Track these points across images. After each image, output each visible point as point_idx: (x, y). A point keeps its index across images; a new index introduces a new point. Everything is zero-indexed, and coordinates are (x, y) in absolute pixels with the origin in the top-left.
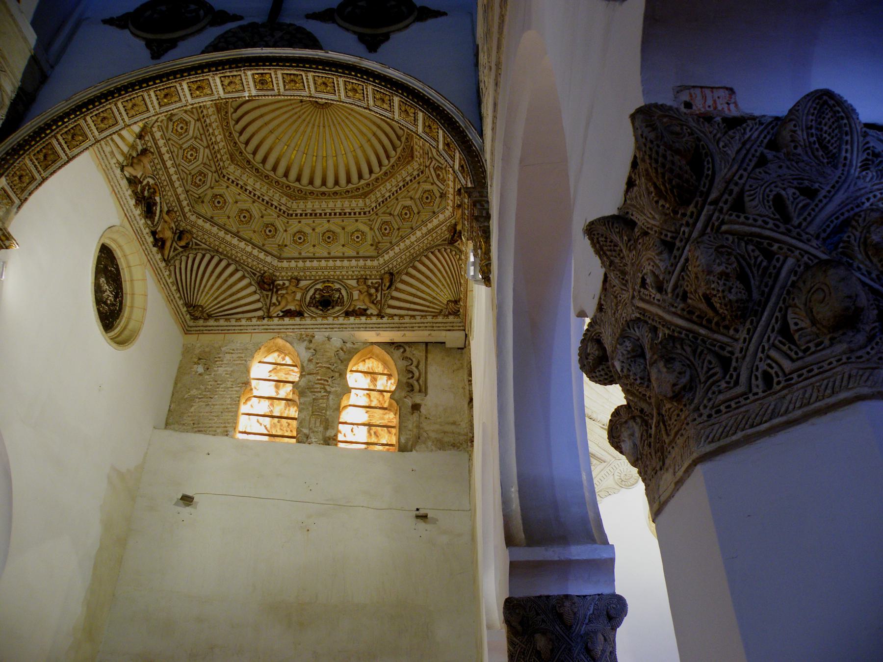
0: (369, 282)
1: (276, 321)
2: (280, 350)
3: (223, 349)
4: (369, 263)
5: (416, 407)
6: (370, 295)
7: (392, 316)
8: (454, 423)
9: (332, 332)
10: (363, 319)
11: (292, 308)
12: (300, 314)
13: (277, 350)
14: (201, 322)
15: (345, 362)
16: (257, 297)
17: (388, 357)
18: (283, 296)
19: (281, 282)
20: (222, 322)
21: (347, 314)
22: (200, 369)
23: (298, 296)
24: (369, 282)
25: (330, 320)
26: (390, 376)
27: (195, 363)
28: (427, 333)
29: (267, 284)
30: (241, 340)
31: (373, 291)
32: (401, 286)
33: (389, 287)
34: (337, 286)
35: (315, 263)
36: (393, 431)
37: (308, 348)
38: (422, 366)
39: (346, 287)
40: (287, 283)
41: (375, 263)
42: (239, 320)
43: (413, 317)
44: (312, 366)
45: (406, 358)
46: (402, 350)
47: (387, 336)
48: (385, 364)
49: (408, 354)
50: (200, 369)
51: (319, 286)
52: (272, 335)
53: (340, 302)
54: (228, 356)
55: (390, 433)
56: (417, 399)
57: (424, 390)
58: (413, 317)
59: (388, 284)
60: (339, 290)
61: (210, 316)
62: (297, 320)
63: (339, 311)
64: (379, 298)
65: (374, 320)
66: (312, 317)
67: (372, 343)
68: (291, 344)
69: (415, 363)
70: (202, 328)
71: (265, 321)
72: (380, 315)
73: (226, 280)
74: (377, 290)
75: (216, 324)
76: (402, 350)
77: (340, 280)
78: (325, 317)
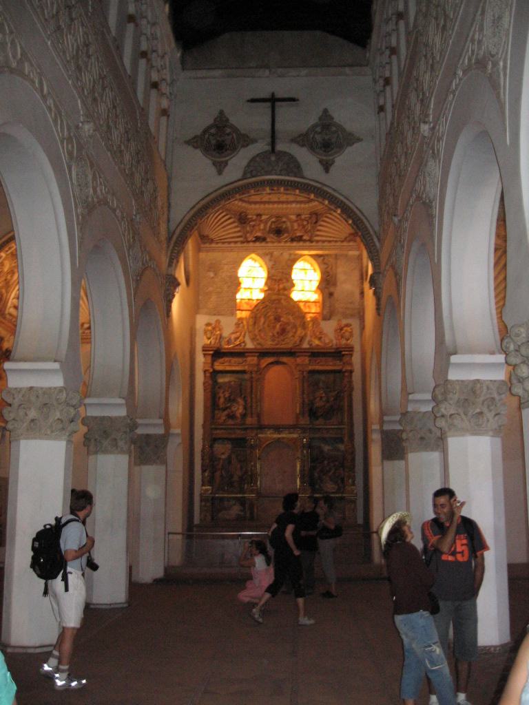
0: (303, 217)
1: (251, 244)
4: (303, 206)
5: (331, 294)
6: (304, 227)
7: (317, 241)
8: (351, 303)
9: (280, 249)
10: (301, 244)
11: (259, 234)
12: (264, 240)
13: (250, 258)
14: (207, 245)
15: (290, 267)
16: (238, 229)
18: (254, 226)
19: (250, 216)
20: (219, 245)
21: (292, 240)
22: (212, 274)
23: (262, 226)
24: (303, 217)
25: (282, 244)
29: (243, 219)
30: (232, 256)
31: (305, 223)
32: (322, 223)
33: (316, 222)
34: (284, 219)
35: (271, 206)
36: (318, 304)
37: (270, 260)
39: (290, 220)
40: (255, 217)
41: (307, 205)
42: (230, 243)
43: (330, 241)
44: (273, 271)
46: (322, 258)
48: (312, 265)
49: (326, 261)
50: (212, 274)
51: (273, 220)
53: (286, 231)
54: (226, 267)
55: (316, 305)
56: (332, 289)
57: (335, 284)
58: (330, 241)
59: (314, 221)
60: (284, 222)
61: (212, 241)
62: (263, 244)
63: (286, 238)
64: (309, 228)
65: (308, 244)
66: (273, 242)
71: (245, 245)
72: (311, 241)
73: (220, 219)
74: (308, 223)
75: (217, 246)
77: (286, 215)
78: (280, 242)
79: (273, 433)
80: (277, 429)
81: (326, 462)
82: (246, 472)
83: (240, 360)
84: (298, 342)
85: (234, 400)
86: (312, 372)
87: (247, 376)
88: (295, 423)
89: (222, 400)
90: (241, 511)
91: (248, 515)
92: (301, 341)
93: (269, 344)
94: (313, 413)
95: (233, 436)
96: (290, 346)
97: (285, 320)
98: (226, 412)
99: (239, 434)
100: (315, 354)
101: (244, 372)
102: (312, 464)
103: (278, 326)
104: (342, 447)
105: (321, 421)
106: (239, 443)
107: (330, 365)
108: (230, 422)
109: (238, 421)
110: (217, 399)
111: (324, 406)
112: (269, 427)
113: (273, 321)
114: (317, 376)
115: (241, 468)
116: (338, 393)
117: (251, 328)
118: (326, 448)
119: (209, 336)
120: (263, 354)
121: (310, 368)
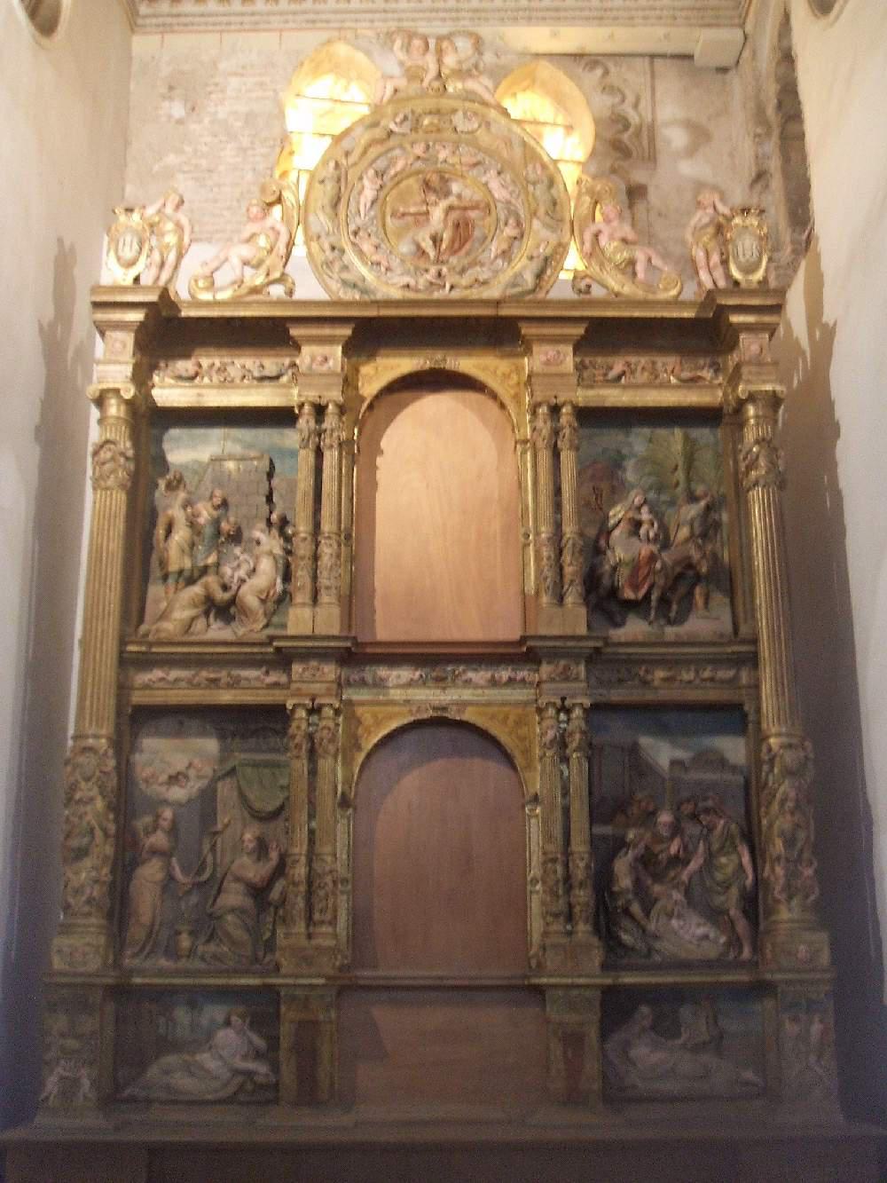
2: (338, 68)
3: (222, 66)
17: (568, 86)
22: (178, 110)
26: (569, 128)
27: (164, 97)
28: (660, 31)
38: (645, 104)
45: (608, 89)
46: (599, 72)
47: (572, 38)
48: (559, 100)
49: (614, 78)
52: (324, 35)
54: (234, 82)
56: (639, 176)
57: (651, 158)
67: (537, 56)
68: (368, 53)
69: (630, 98)
70: (169, 20)
76: (599, 72)
79: (410, 684)
80: (435, 659)
81: (665, 818)
82: (280, 870)
83: (271, 363)
84: (529, 279)
85: (236, 537)
86: (590, 417)
87: (290, 438)
88: (515, 634)
89: (181, 535)
90: (258, 1055)
91: (288, 1074)
92: (539, 276)
93: (390, 281)
94: (604, 599)
95: (226, 697)
96: (493, 292)
97: (467, 193)
98: (197, 590)
99: (254, 687)
100: (607, 334)
101: (282, 417)
102: (601, 830)
103: (437, 214)
104: (734, 749)
105: (634, 628)
106: (257, 724)
107: (659, 383)
108: (218, 630)
109: (251, 629)
110: (160, 531)
111: (652, 558)
112: (396, 655)
113: (419, 197)
114: (611, 438)
115: (262, 848)
116: (708, 508)
117: (320, 220)
118: (662, 753)
119: (128, 254)
120: (371, 332)
121: (584, 397)
